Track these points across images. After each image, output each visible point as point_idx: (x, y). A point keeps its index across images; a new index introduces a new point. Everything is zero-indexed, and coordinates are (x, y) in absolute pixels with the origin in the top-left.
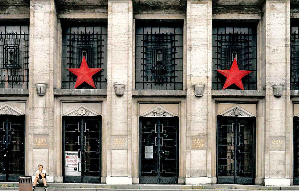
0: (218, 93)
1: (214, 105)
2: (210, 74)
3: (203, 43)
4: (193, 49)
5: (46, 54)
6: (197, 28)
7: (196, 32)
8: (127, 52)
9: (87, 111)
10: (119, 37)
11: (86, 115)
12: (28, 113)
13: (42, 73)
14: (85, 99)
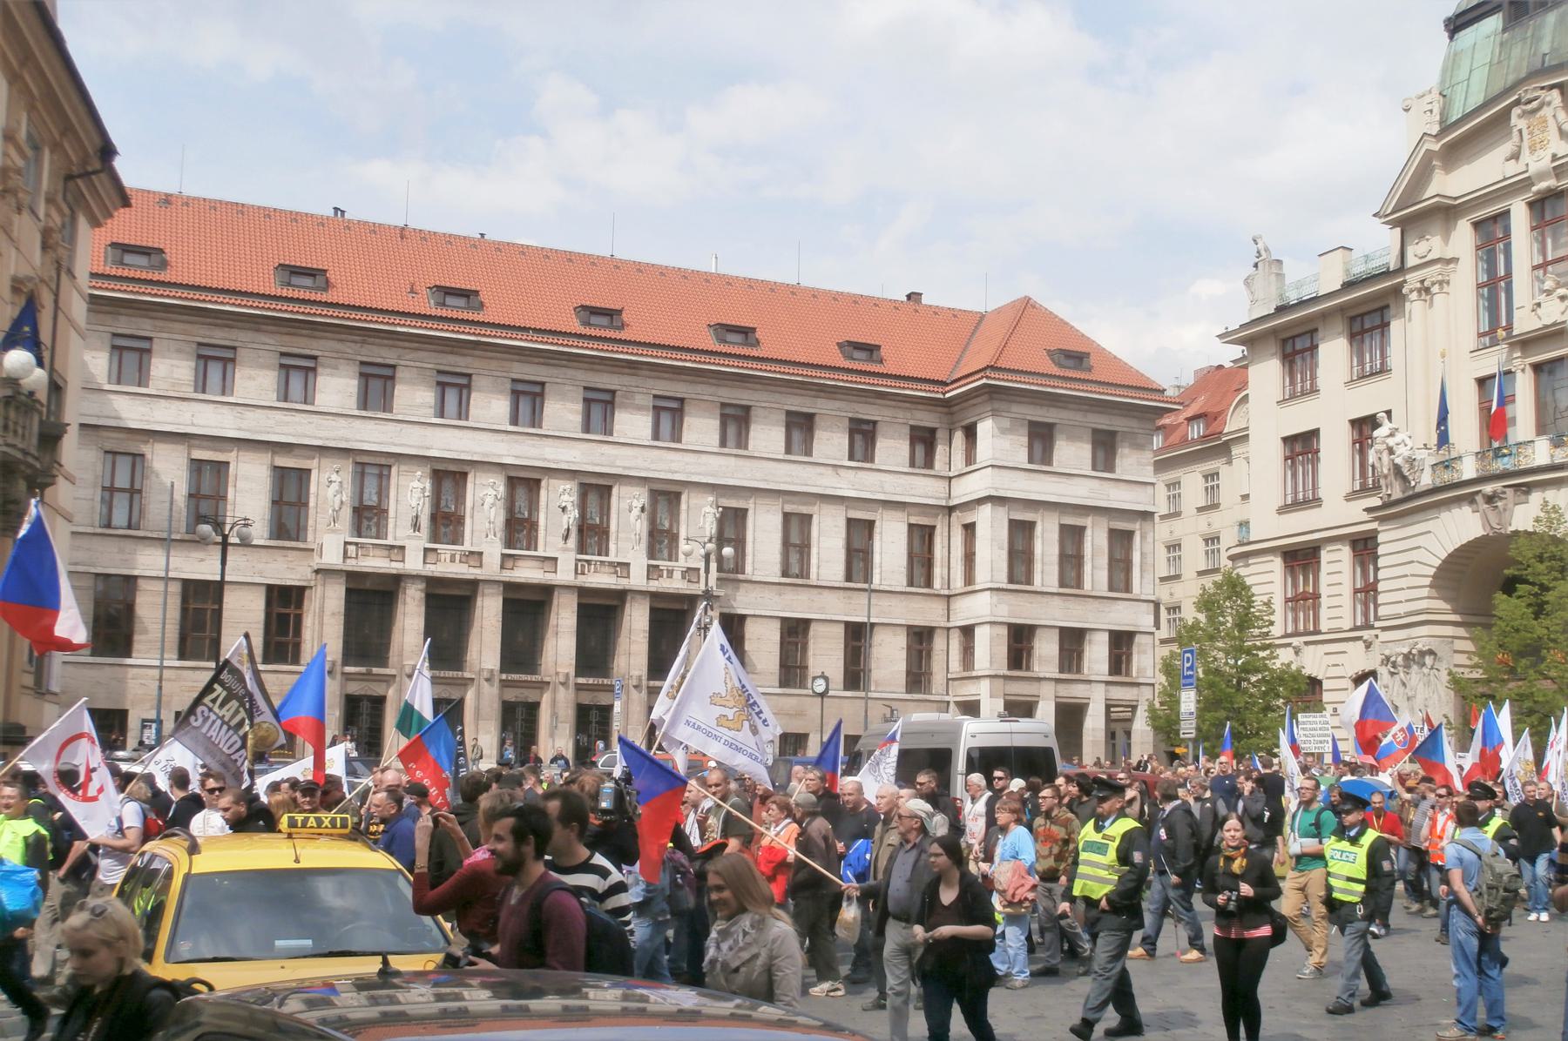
0: (581, 680)
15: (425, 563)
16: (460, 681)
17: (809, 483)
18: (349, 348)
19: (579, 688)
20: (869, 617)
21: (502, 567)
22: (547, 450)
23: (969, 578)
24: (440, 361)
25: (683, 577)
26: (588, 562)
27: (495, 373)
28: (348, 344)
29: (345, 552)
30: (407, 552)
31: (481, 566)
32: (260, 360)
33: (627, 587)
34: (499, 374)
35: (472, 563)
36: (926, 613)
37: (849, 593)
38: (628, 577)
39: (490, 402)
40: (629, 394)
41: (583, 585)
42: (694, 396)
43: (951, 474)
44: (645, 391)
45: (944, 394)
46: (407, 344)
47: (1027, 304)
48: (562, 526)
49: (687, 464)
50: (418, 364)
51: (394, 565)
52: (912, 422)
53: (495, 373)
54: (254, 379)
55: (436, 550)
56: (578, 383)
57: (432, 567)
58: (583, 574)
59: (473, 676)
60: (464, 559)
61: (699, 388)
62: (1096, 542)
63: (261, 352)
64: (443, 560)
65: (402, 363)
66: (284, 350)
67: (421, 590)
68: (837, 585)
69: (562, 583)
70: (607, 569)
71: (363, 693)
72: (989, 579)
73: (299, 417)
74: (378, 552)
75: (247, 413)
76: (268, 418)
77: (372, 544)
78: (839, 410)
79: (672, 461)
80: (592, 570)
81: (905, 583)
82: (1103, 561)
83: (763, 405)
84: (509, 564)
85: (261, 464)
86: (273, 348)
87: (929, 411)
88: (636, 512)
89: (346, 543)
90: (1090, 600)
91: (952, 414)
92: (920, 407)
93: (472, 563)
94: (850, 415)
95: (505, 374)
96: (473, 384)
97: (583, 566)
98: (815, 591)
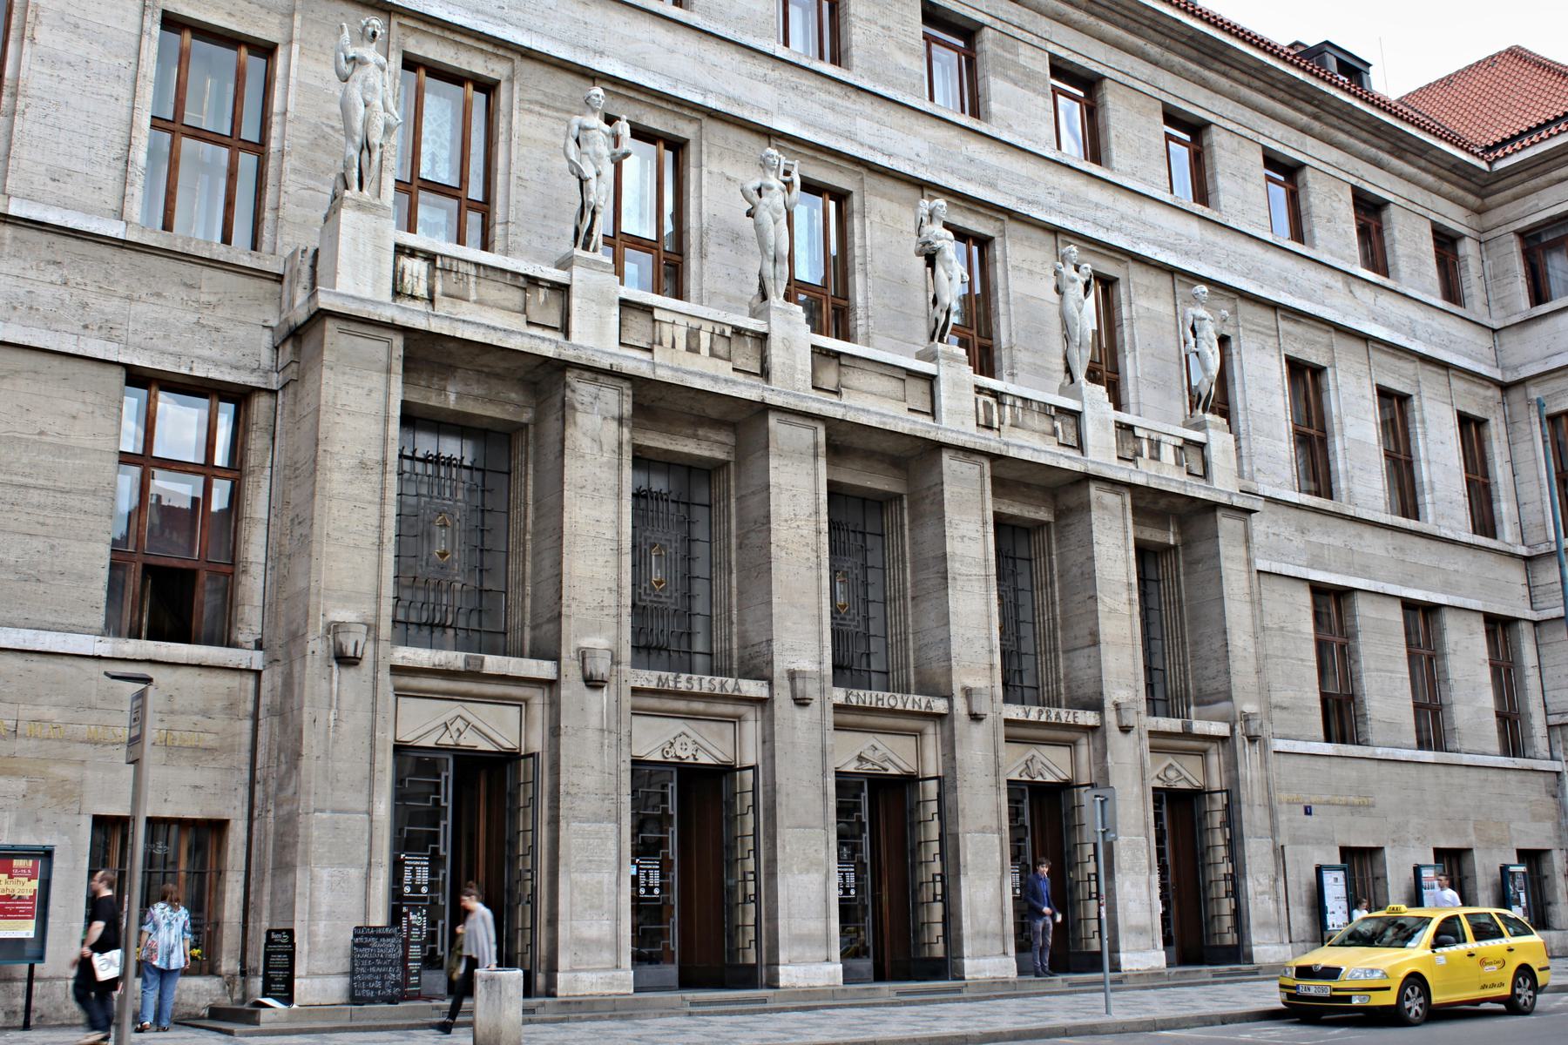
5: (607, 548)
7: (962, 537)
8: (814, 573)
9: (698, 747)
10: (794, 525)
11: (691, 760)
13: (597, 612)
16: (728, 709)
25: (1179, 464)
29: (398, 276)
30: (575, 302)
42: (1119, 77)
44: (1036, 41)
55: (648, 309)
58: (989, 427)
59: (764, 693)
60: (721, 347)
64: (667, 340)
71: (447, 740)
74: (492, 291)
77: (477, 265)
79: (1096, 204)
80: (1008, 421)
84: (829, 377)
89: (400, 250)
92: (1446, 187)
94: (1353, 181)
97: (986, 404)
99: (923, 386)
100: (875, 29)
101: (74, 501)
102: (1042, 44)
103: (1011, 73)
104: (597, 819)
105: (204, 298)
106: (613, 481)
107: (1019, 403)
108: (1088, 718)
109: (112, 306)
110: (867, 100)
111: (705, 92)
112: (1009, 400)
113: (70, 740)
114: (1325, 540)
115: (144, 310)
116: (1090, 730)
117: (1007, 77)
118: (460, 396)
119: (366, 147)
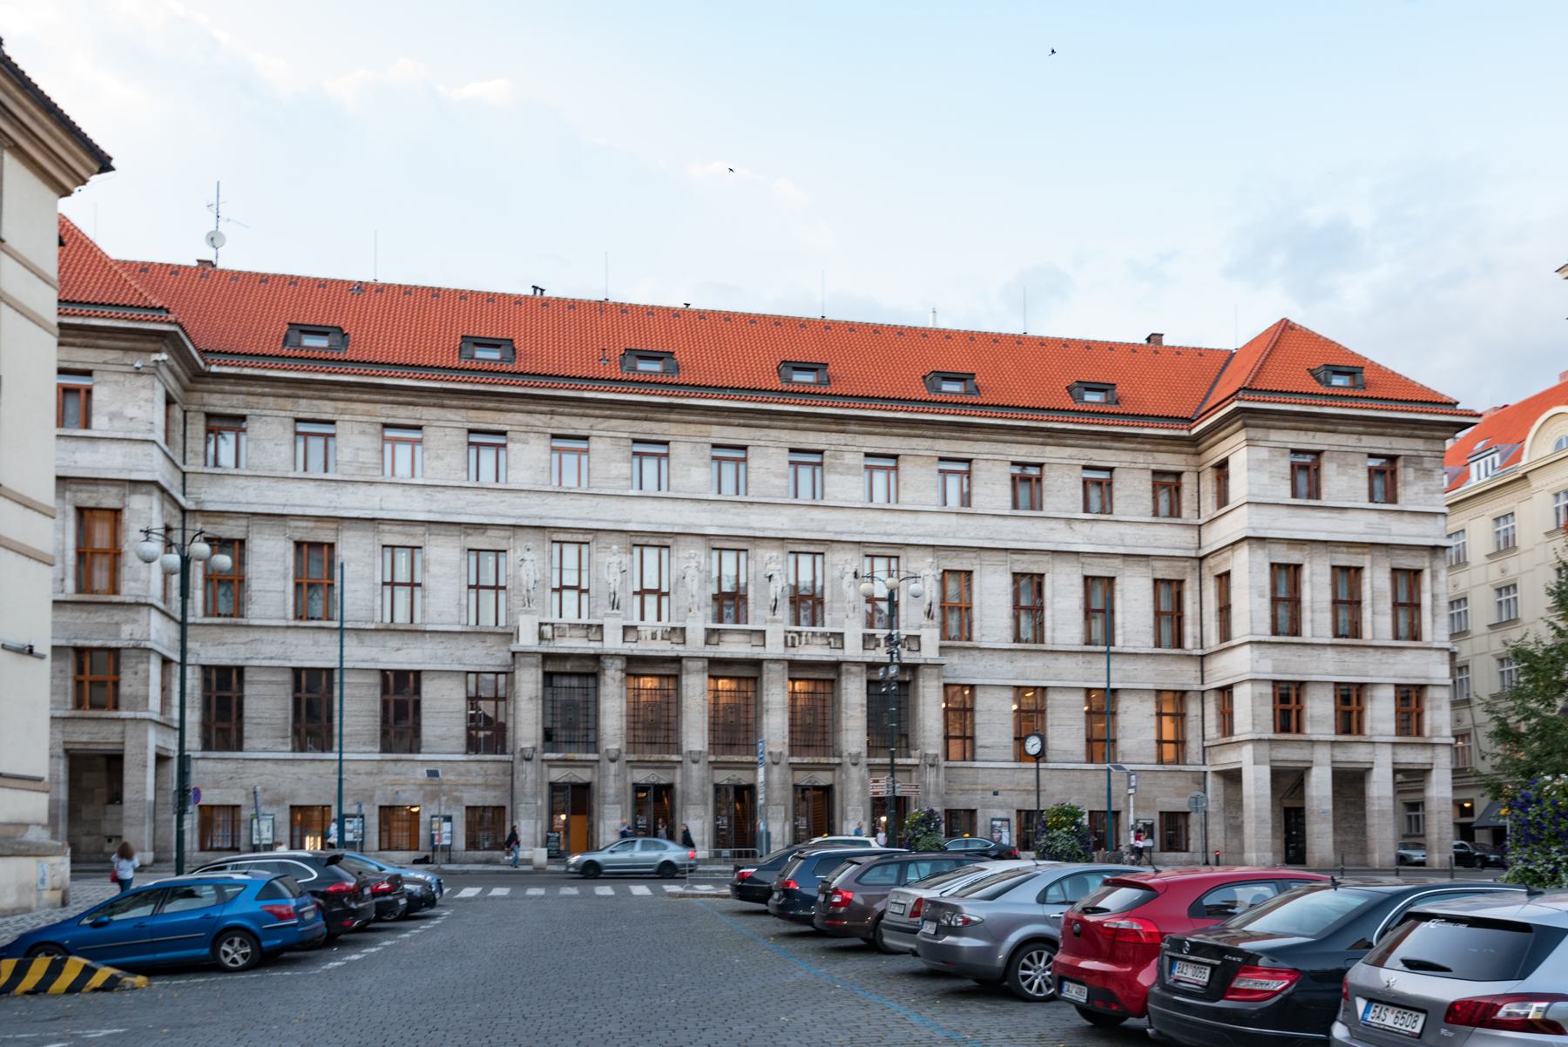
0: (795, 760)
1: (790, 772)
2: (787, 740)
3: (778, 707)
4: (770, 713)
6: (773, 691)
12: (596, 779)
14: (657, 765)
15: (624, 641)
17: (1041, 538)
18: (537, 420)
19: (795, 767)
20: (1109, 682)
21: (707, 643)
22: (753, 517)
23: (1225, 634)
24: (634, 429)
26: (799, 633)
27: (694, 439)
28: (537, 416)
30: (605, 630)
31: (684, 643)
32: (448, 438)
33: (841, 659)
34: (698, 439)
35: (674, 640)
36: (1182, 676)
37: (1089, 658)
38: (843, 648)
39: (689, 470)
40: (838, 453)
41: (793, 658)
42: (909, 452)
43: (1201, 522)
44: (855, 449)
45: (1190, 431)
46: (597, 412)
47: (1286, 327)
48: (769, 597)
49: (904, 525)
50: (611, 434)
51: (592, 644)
52: (1154, 467)
53: (694, 439)
54: (442, 459)
55: (635, 627)
56: (781, 444)
57: (633, 646)
58: (793, 646)
59: (680, 759)
60: (666, 636)
61: (914, 442)
62: (1376, 583)
63: (447, 430)
64: (643, 638)
65: (595, 433)
66: (471, 426)
67: (622, 670)
68: (1074, 649)
69: (770, 657)
70: (819, 641)
71: (567, 780)
72: (1249, 631)
73: (490, 497)
74: (575, 632)
75: (437, 494)
76: (460, 499)
78: (1071, 458)
79: (888, 523)
80: (803, 642)
81: (1152, 644)
82: (1386, 605)
83: (986, 457)
84: (714, 639)
85: (454, 547)
86: (460, 425)
87: (1174, 452)
88: (849, 577)
89: (541, 624)
90: (1370, 650)
91: (1199, 454)
92: (1162, 448)
93: (674, 640)
95: (703, 440)
96: (671, 452)
98: (1049, 657)
99: (761, 635)
100: (761, 471)
101: (454, 715)
102: (860, 449)
103: (839, 470)
104: (614, 803)
105: (488, 644)
106: (619, 691)
107: (810, 634)
108: (837, 760)
109: (459, 653)
110: (756, 506)
111: (674, 525)
112: (804, 634)
113: (457, 785)
114: (1029, 664)
115: (470, 652)
116: (839, 764)
117: (836, 473)
118: (572, 667)
119: (528, 591)
